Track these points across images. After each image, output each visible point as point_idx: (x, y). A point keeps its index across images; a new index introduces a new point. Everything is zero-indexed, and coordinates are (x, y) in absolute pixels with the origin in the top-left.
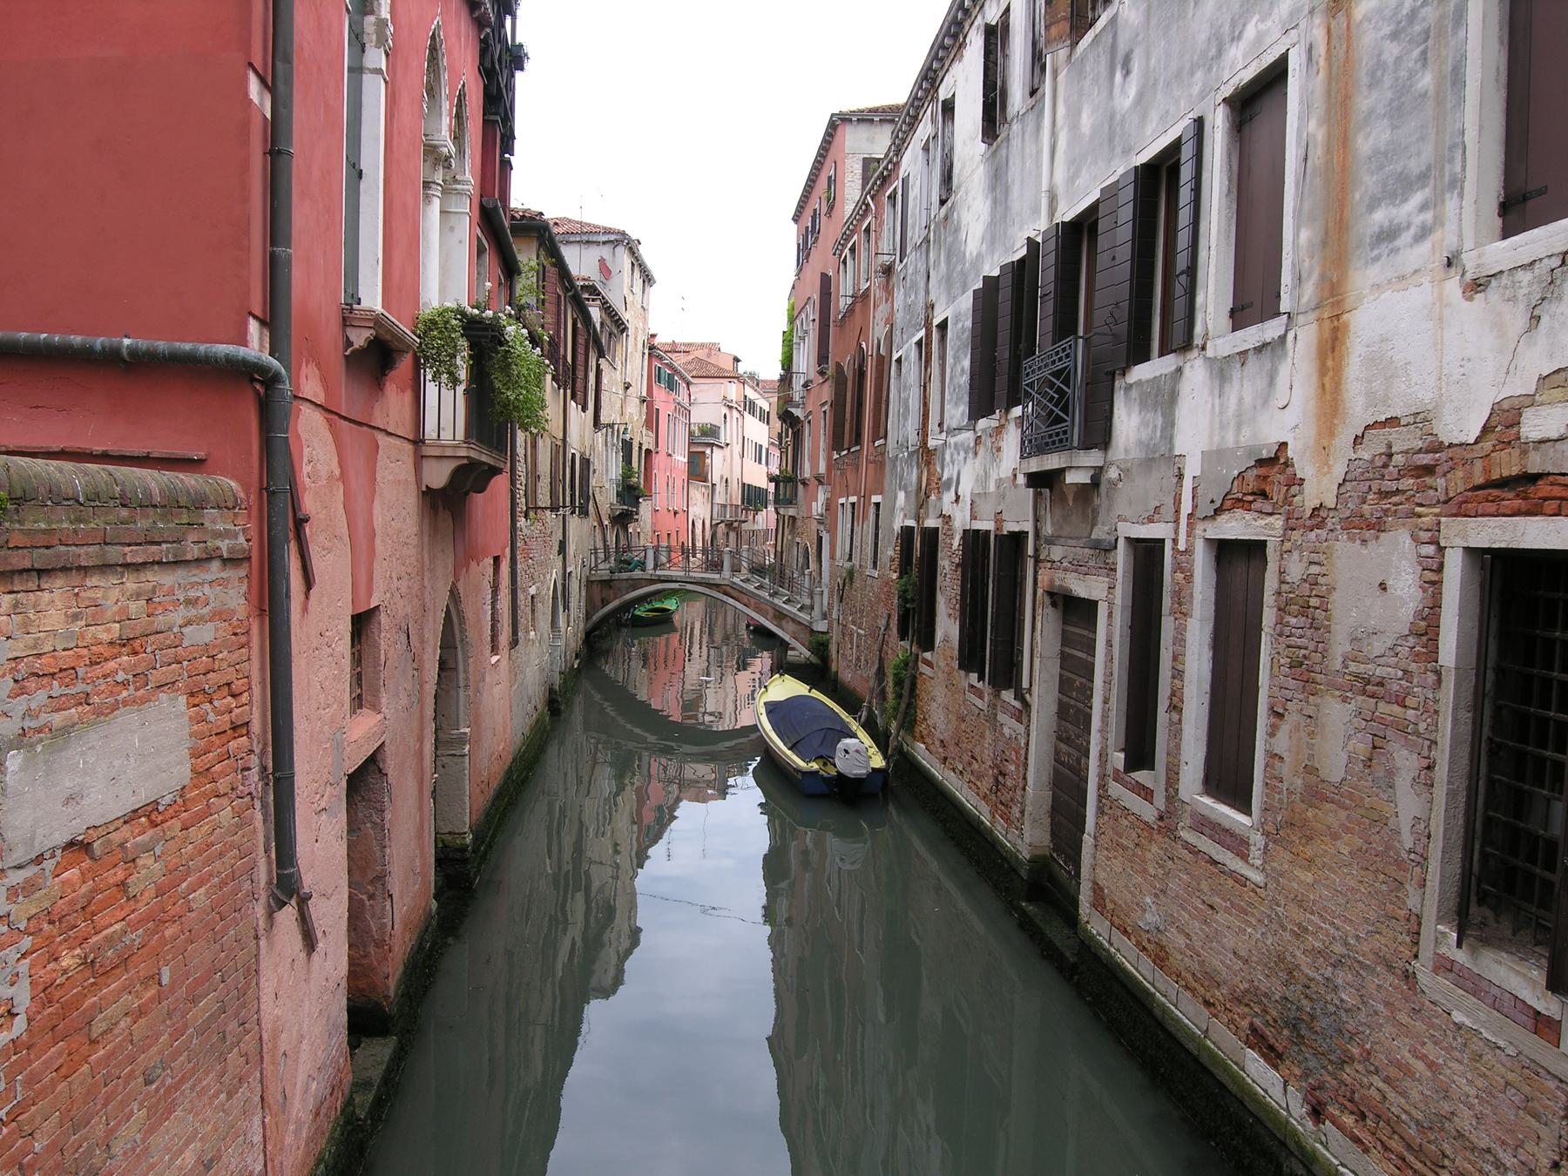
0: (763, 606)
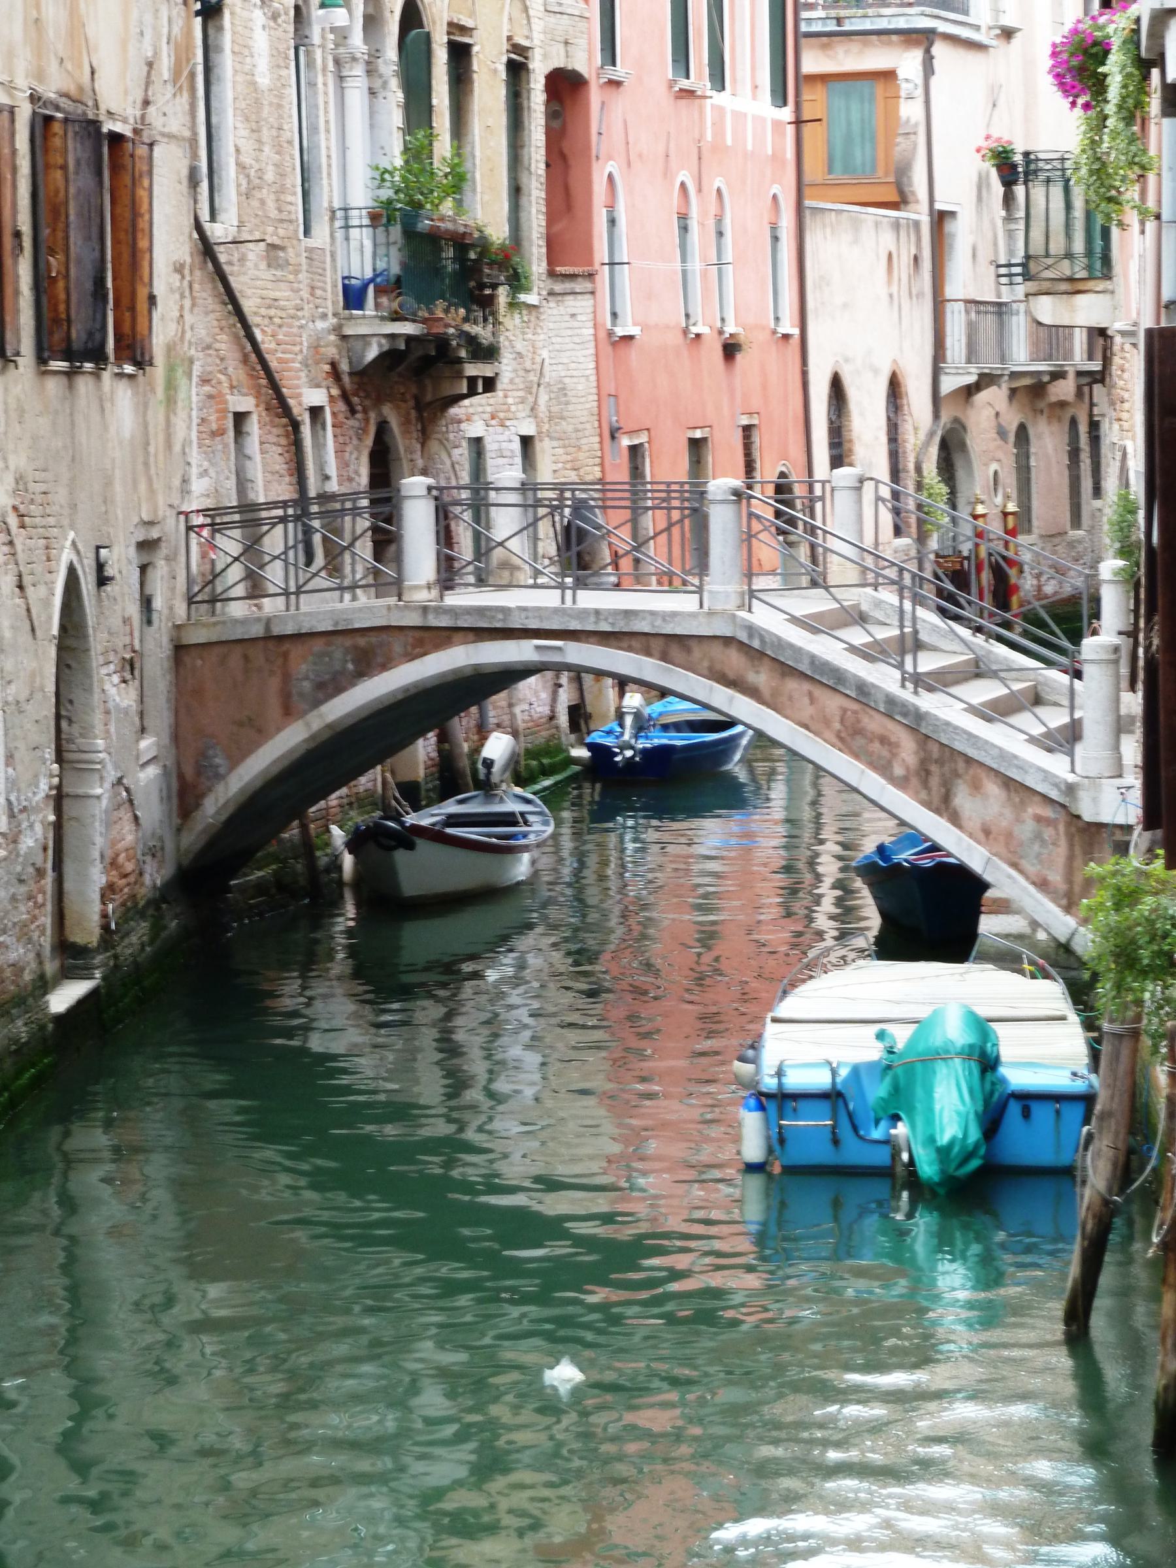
0: (874, 723)
